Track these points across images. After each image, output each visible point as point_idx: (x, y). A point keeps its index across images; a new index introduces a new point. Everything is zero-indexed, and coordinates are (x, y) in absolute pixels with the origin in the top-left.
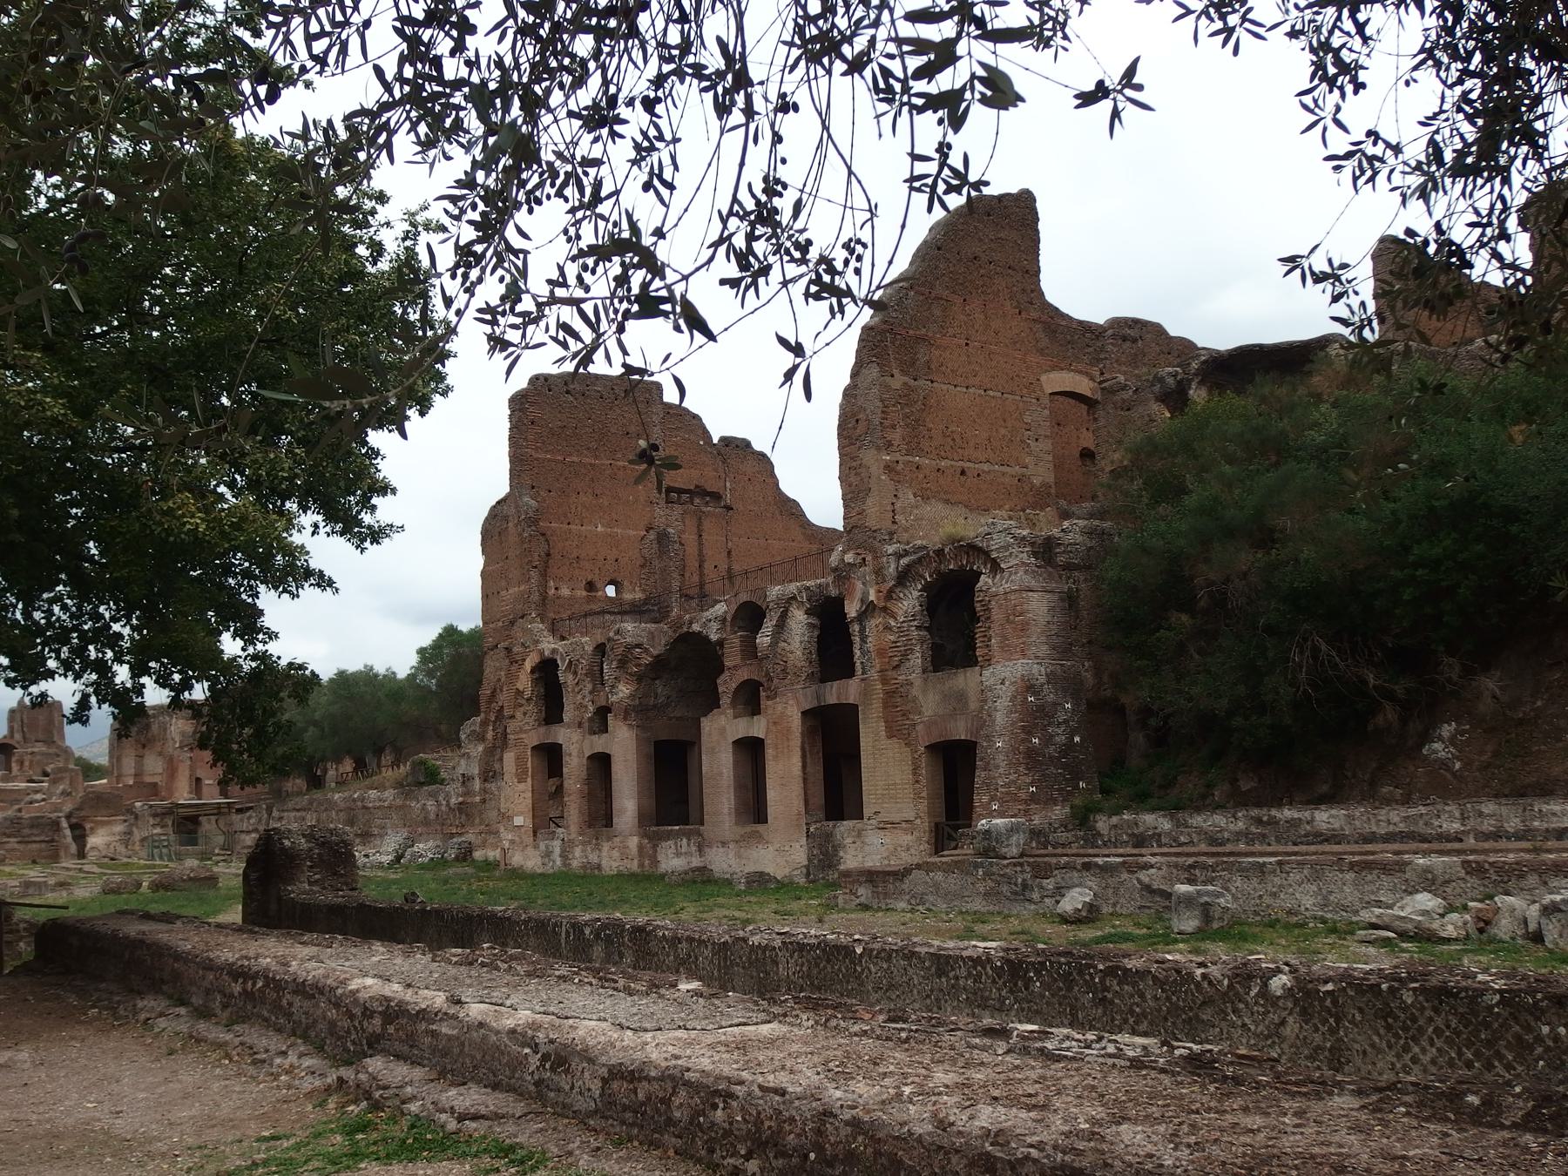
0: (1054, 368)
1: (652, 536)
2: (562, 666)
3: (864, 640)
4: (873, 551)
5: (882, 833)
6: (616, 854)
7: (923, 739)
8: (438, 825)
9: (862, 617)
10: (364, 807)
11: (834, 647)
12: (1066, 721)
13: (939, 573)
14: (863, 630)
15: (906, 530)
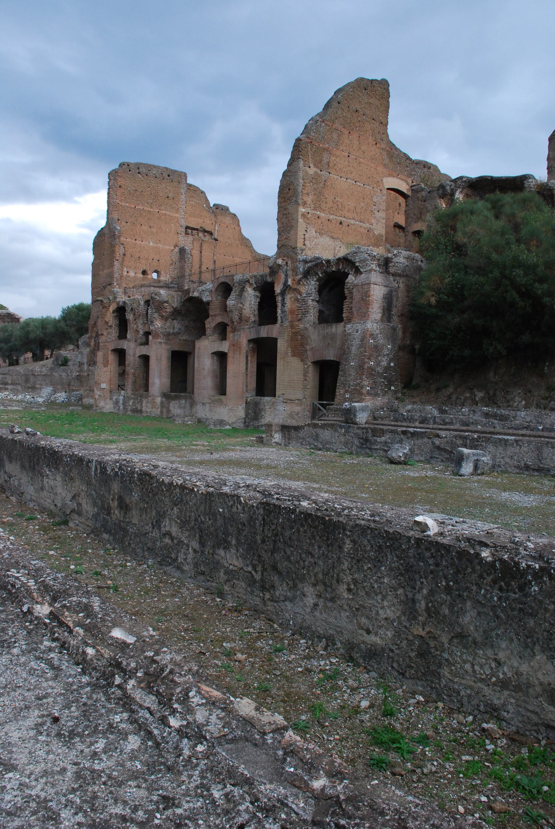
0: (390, 175)
1: (177, 250)
2: (128, 309)
3: (283, 305)
4: (292, 258)
5: (285, 405)
6: (150, 405)
7: (311, 357)
8: (68, 387)
9: (283, 293)
10: (33, 375)
11: (268, 309)
12: (388, 355)
13: (325, 272)
14: (283, 299)
15: (310, 249)
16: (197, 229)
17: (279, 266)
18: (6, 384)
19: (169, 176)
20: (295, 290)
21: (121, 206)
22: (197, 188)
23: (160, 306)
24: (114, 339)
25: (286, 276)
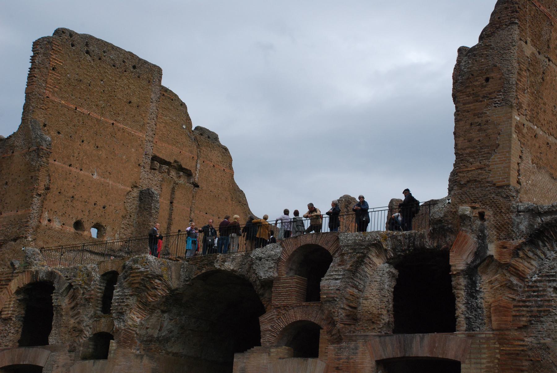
1: (135, 193)
2: (60, 287)
9: (471, 272)
16: (168, 164)
17: (464, 218)
19: (134, 67)
20: (507, 266)
21: (52, 102)
22: (176, 95)
23: (143, 284)
24: (11, 345)
25: (482, 238)
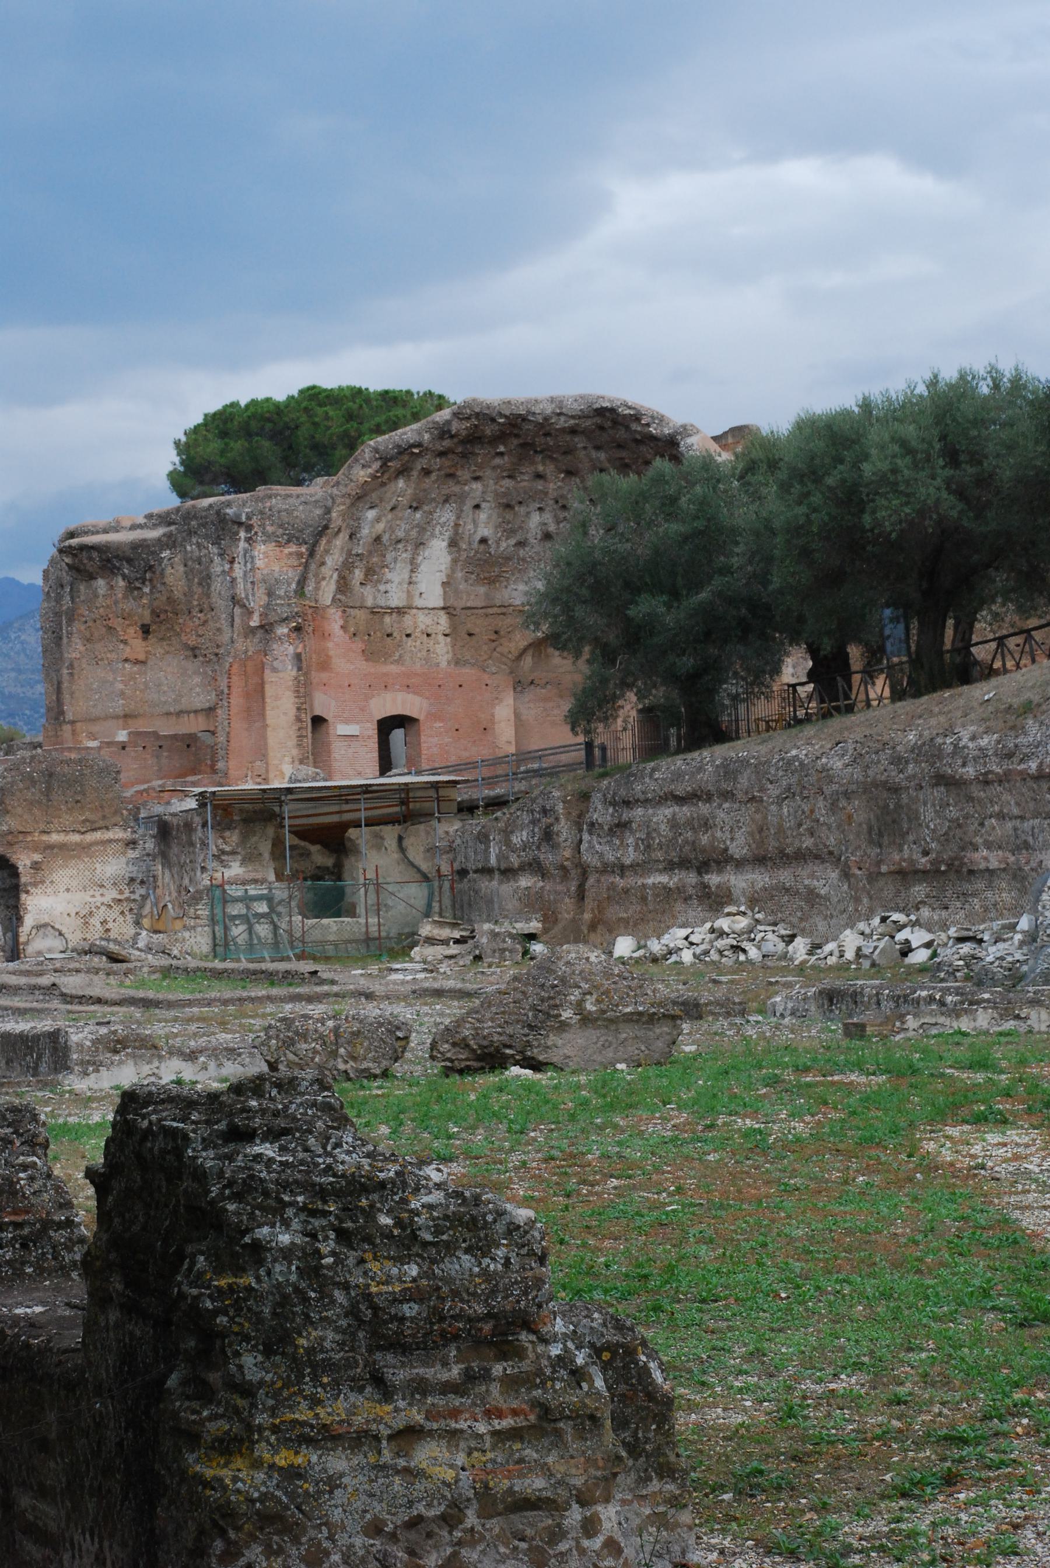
10: (942, 780)
18: (719, 860)
